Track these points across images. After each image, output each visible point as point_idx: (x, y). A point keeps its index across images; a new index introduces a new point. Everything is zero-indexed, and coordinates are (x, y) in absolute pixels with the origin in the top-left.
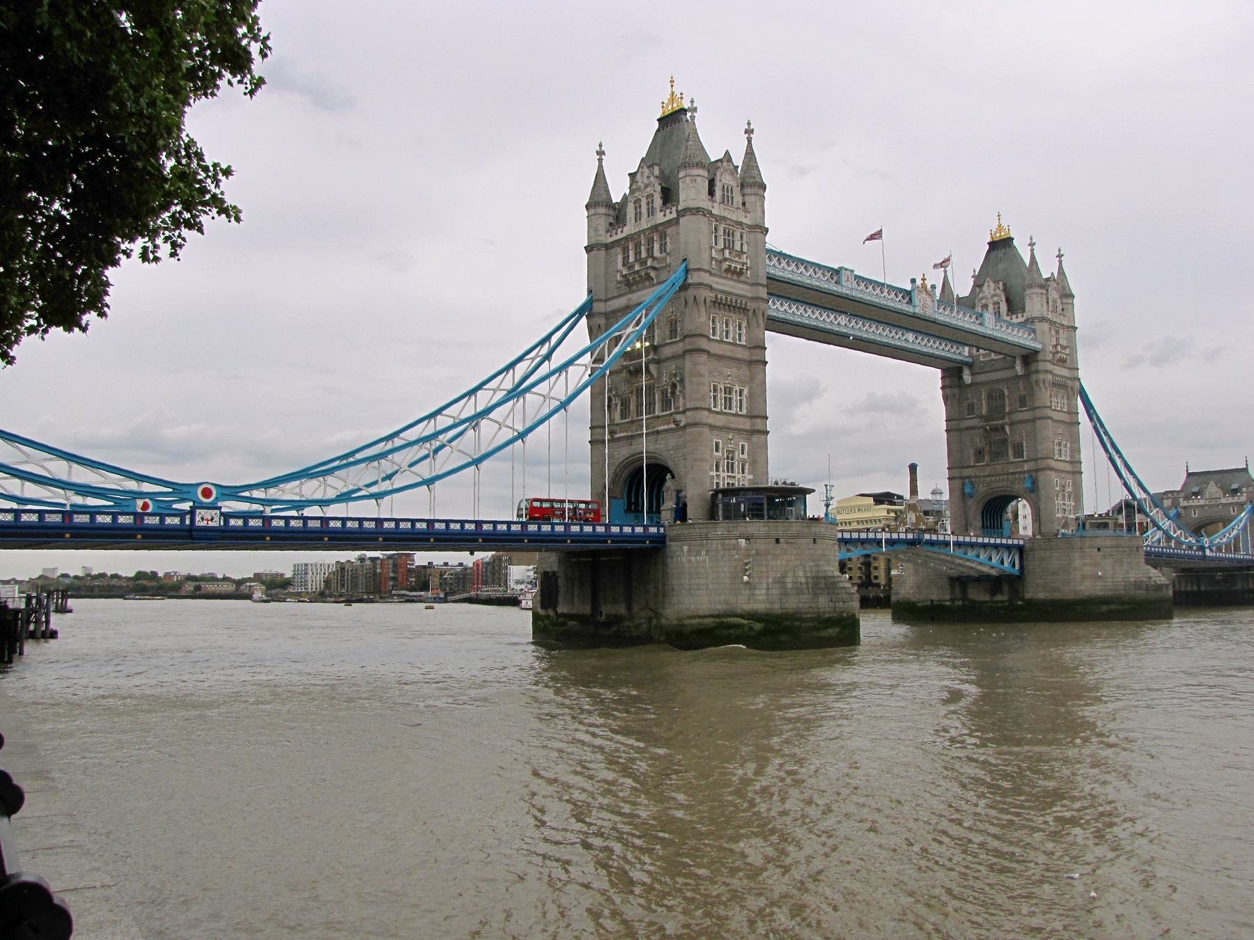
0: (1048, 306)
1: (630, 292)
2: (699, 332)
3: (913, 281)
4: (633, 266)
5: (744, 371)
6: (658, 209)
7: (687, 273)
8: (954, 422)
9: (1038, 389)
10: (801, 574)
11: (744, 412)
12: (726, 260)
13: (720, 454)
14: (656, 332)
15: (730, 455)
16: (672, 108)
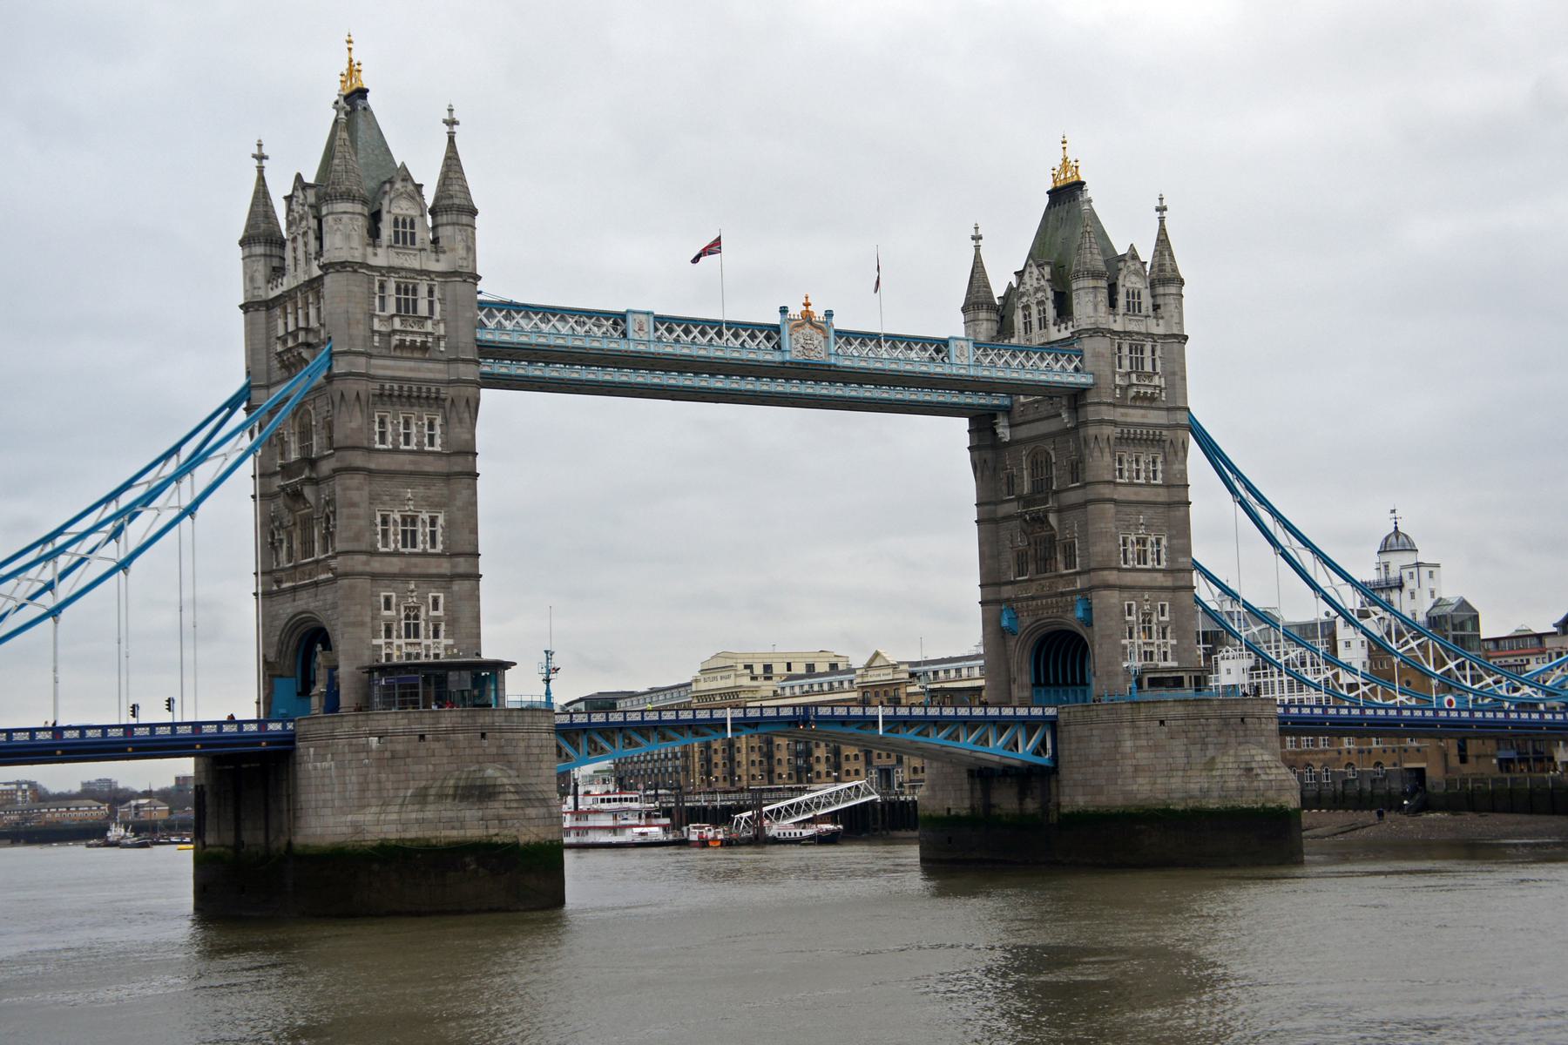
0: (1112, 303)
1: (290, 378)
2: (349, 443)
3: (784, 310)
4: (285, 342)
5: (438, 489)
6: (313, 256)
7: (331, 359)
8: (987, 508)
9: (1087, 452)
10: (452, 782)
11: (439, 548)
12: (394, 332)
13: (392, 613)
14: (315, 437)
15: (412, 614)
16: (351, 85)
